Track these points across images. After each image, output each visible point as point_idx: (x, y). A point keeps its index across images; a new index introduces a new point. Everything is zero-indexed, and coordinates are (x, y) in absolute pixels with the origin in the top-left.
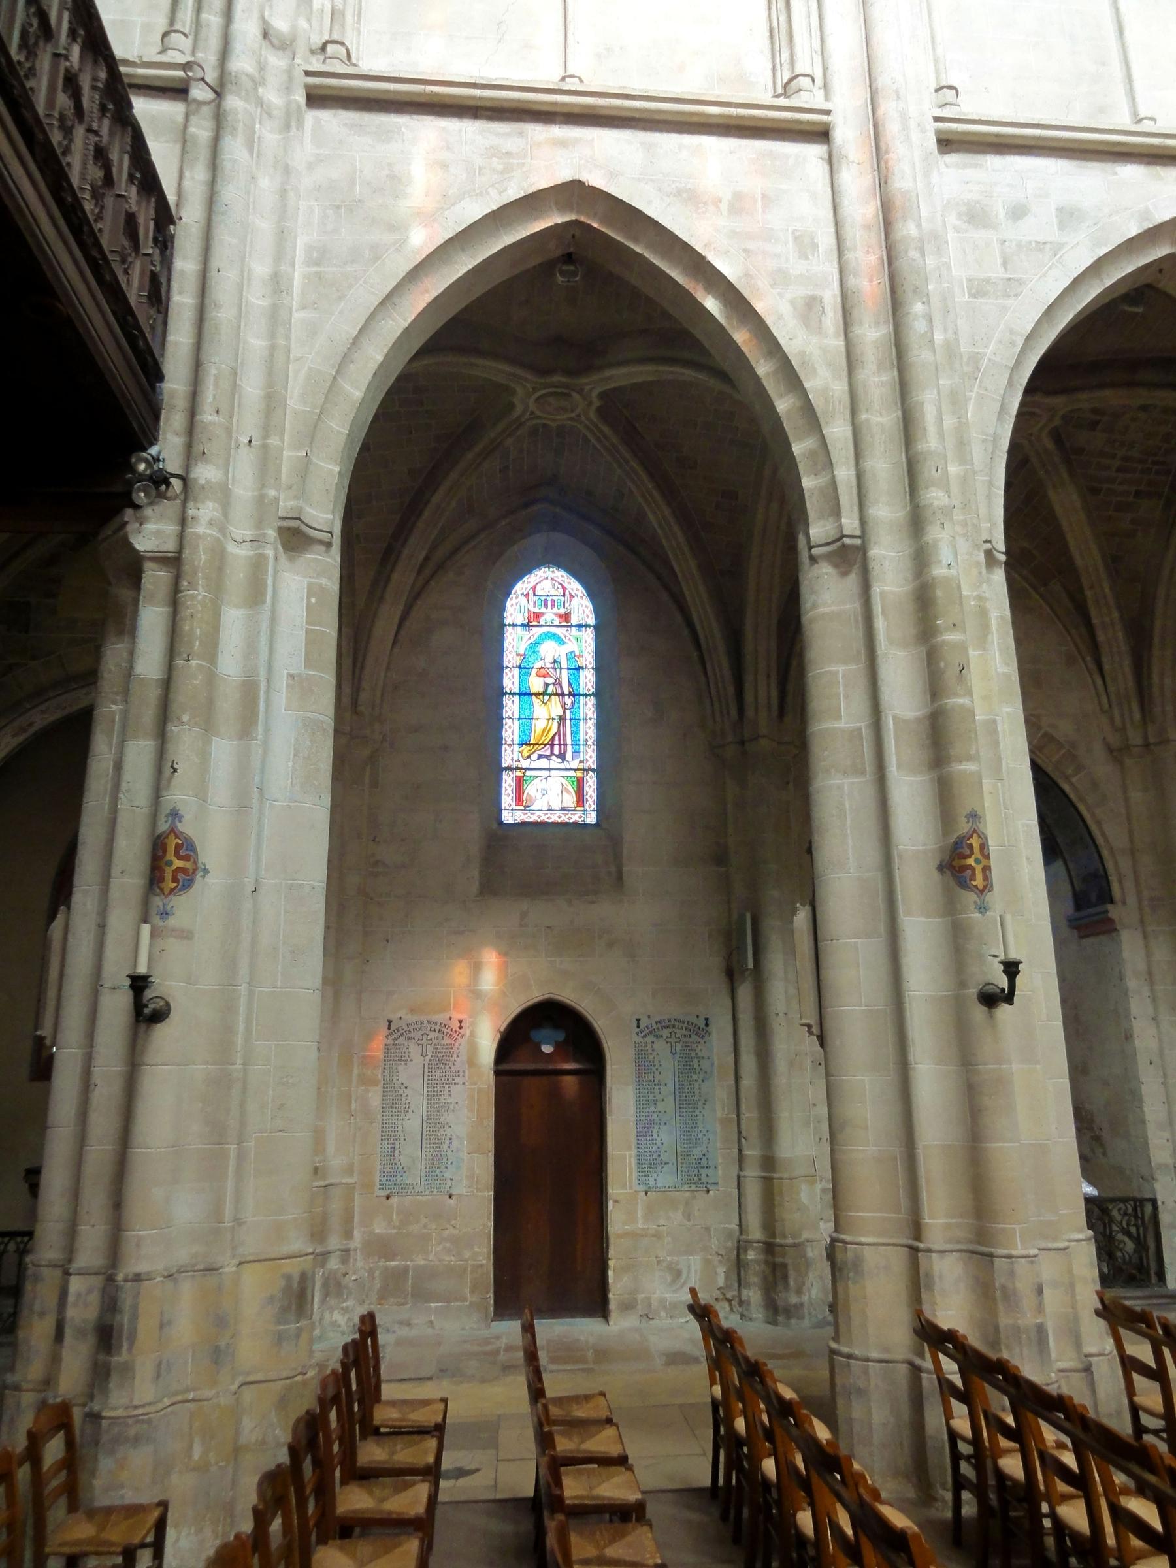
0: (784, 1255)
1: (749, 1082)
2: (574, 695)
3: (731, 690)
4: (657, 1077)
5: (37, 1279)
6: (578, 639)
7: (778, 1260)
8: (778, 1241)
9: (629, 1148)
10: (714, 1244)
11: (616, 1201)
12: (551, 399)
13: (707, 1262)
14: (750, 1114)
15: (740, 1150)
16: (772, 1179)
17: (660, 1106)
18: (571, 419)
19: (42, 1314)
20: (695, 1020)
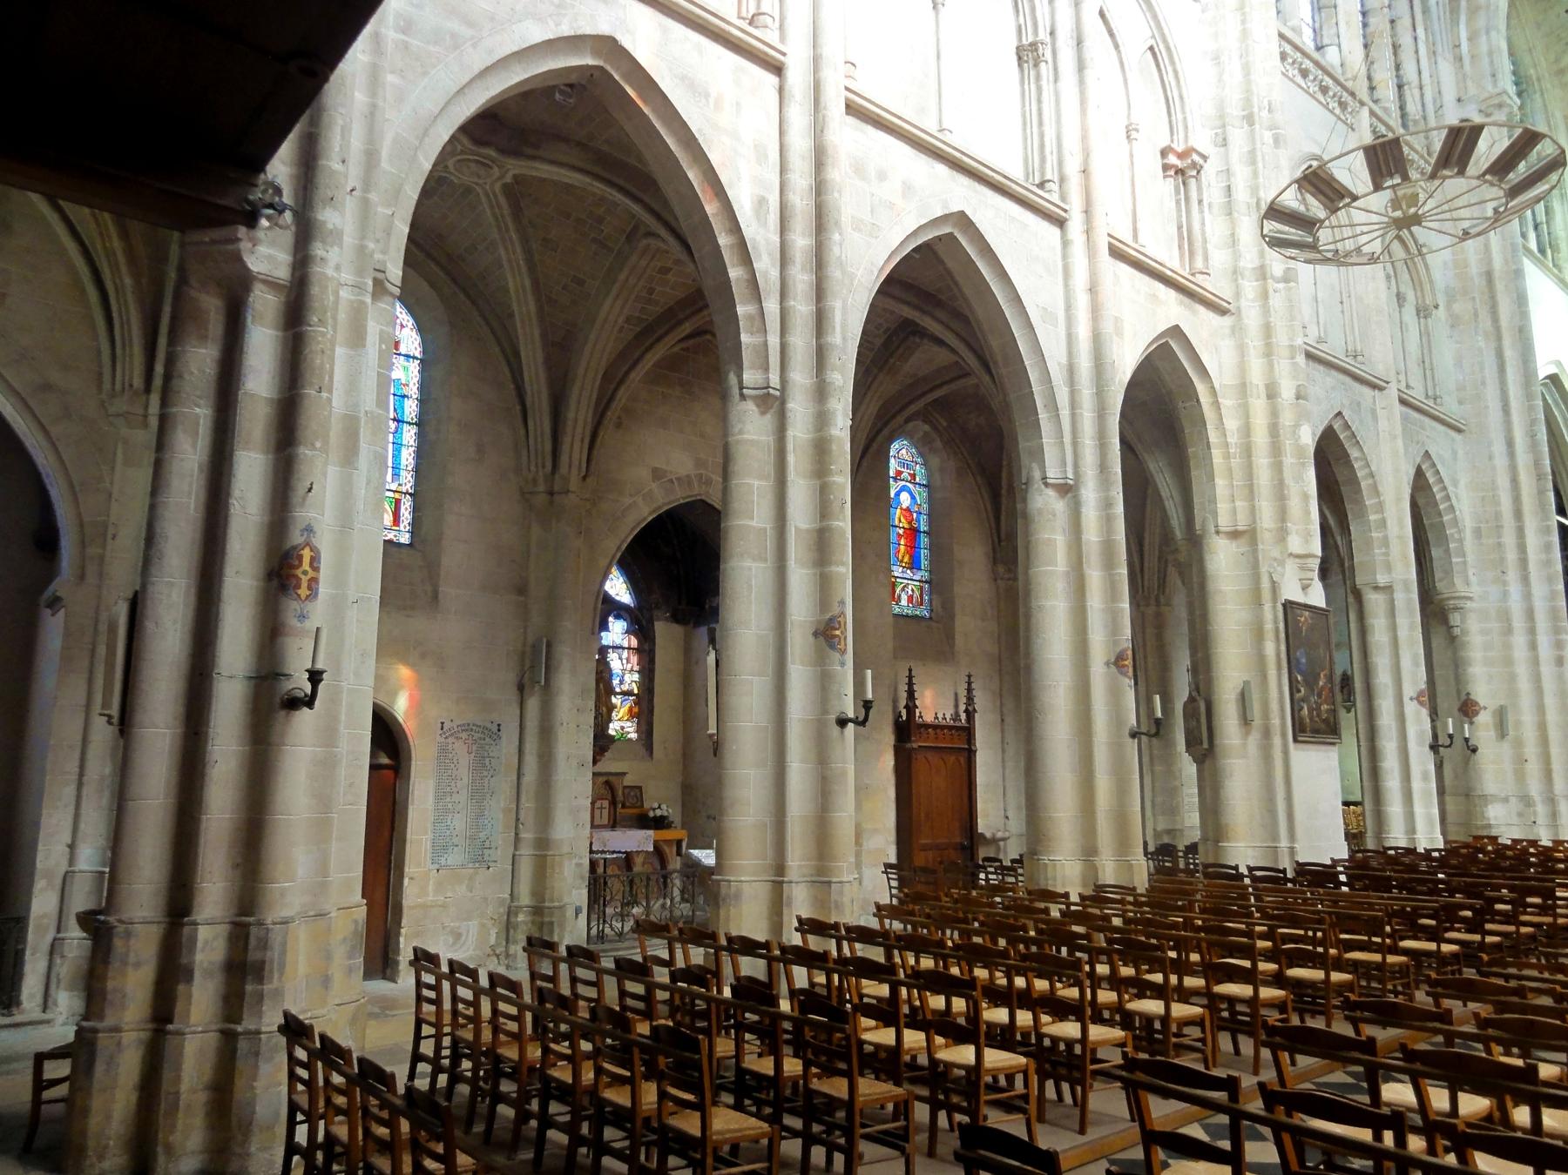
0: (552, 915)
1: (530, 776)
2: (398, 421)
3: (548, 447)
4: (455, 772)
5: (128, 935)
6: (406, 369)
7: (547, 919)
8: (547, 904)
9: (426, 833)
10: (490, 911)
11: (411, 878)
12: (472, 165)
13: (483, 926)
14: (528, 803)
15: (517, 834)
16: (546, 856)
17: (456, 798)
18: (477, 184)
19: (138, 965)
20: (489, 725)
